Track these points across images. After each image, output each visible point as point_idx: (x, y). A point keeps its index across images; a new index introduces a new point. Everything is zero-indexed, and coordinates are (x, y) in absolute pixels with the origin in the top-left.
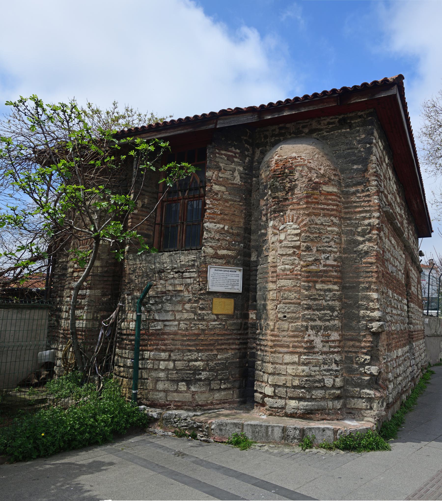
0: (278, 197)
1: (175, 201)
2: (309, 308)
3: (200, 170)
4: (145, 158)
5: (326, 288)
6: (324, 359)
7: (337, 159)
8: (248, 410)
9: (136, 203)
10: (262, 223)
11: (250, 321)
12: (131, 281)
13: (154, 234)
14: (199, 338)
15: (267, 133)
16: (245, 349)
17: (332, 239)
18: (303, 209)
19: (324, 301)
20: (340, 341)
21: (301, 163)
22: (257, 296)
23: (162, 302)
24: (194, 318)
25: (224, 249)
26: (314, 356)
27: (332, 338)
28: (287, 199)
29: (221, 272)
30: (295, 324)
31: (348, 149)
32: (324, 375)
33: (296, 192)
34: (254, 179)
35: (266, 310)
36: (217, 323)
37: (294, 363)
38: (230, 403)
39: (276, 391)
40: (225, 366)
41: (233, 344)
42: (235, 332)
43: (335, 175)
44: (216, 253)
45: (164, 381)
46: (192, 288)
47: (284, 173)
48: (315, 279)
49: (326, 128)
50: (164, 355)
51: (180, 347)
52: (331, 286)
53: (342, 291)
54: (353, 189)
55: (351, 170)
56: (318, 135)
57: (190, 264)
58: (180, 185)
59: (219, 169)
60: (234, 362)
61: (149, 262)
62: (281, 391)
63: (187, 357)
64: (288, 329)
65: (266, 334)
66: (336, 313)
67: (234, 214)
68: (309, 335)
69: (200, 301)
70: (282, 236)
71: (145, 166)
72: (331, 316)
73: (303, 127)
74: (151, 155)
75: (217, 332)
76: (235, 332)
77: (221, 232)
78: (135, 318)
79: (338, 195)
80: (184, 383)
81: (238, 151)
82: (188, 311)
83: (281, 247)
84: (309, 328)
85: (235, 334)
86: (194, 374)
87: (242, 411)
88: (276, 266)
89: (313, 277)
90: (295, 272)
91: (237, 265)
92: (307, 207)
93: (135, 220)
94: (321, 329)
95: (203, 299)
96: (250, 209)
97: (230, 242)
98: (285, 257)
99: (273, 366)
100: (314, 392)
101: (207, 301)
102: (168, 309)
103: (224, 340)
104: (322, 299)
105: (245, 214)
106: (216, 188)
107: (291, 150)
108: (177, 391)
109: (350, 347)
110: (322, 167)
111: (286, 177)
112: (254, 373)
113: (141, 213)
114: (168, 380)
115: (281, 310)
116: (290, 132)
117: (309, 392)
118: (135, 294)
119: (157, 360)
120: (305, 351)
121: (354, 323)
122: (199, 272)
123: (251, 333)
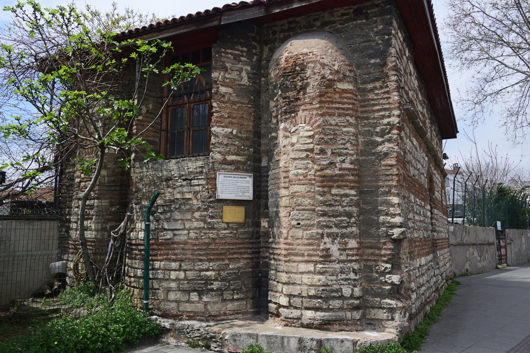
0: (288, 97)
1: (180, 106)
2: (324, 214)
3: (205, 70)
4: (147, 61)
5: (342, 193)
6: (341, 268)
7: (352, 53)
8: (262, 321)
9: (140, 109)
10: (272, 126)
11: (262, 230)
12: (138, 190)
13: (160, 141)
14: (210, 247)
15: (275, 29)
16: (258, 258)
17: (348, 141)
18: (316, 109)
19: (340, 207)
20: (358, 249)
21: (312, 59)
22: (269, 203)
23: (171, 211)
24: (204, 227)
25: (233, 154)
26: (331, 265)
27: (350, 246)
28: (298, 99)
29: (230, 179)
30: (310, 232)
31: (364, 42)
32: (342, 285)
33: (308, 90)
34: (263, 79)
35: (279, 217)
36: (227, 231)
37: (309, 272)
38: (243, 313)
39: (292, 301)
40: (237, 276)
41: (245, 253)
42: (247, 241)
43: (350, 71)
44: (225, 159)
45: (175, 291)
46: (201, 196)
47: (296, 70)
48: (330, 183)
49: (340, 20)
50: (174, 265)
51: (190, 256)
52: (347, 191)
53: (359, 196)
54: (370, 86)
55: (368, 65)
56: (331, 28)
57: (198, 171)
58: (185, 88)
59: (226, 69)
60: (246, 272)
61: (156, 170)
62: (297, 301)
63: (198, 267)
64: (303, 236)
65: (279, 243)
66: (353, 220)
67: (242, 117)
68: (325, 243)
69: (210, 209)
70: (294, 139)
71: (148, 69)
72: (348, 223)
73: (315, 20)
74: (154, 57)
75: (228, 241)
76: (247, 241)
77: (229, 136)
78: (143, 227)
79: (354, 92)
80: (195, 293)
81: (245, 49)
82: (197, 220)
83: (293, 151)
84: (325, 235)
85: (247, 243)
86: (206, 284)
87: (256, 322)
88: (288, 171)
89: (327, 182)
90: (309, 177)
91: (247, 171)
92: (320, 107)
93: (140, 127)
94: (337, 236)
95: (213, 207)
96: (260, 111)
97: (239, 147)
98: (297, 161)
99: (288, 276)
100: (331, 302)
101: (217, 209)
102: (177, 218)
103: (236, 249)
104: (338, 205)
105: (254, 117)
106: (223, 89)
107: (302, 45)
108: (189, 301)
109: (369, 255)
110: (336, 63)
111: (298, 76)
112: (268, 283)
113: (146, 119)
114: (179, 290)
115: (294, 217)
116: (300, 27)
117: (326, 302)
118: (143, 203)
119: (168, 270)
120: (321, 259)
121: (373, 230)
122: (208, 179)
123: (263, 242)
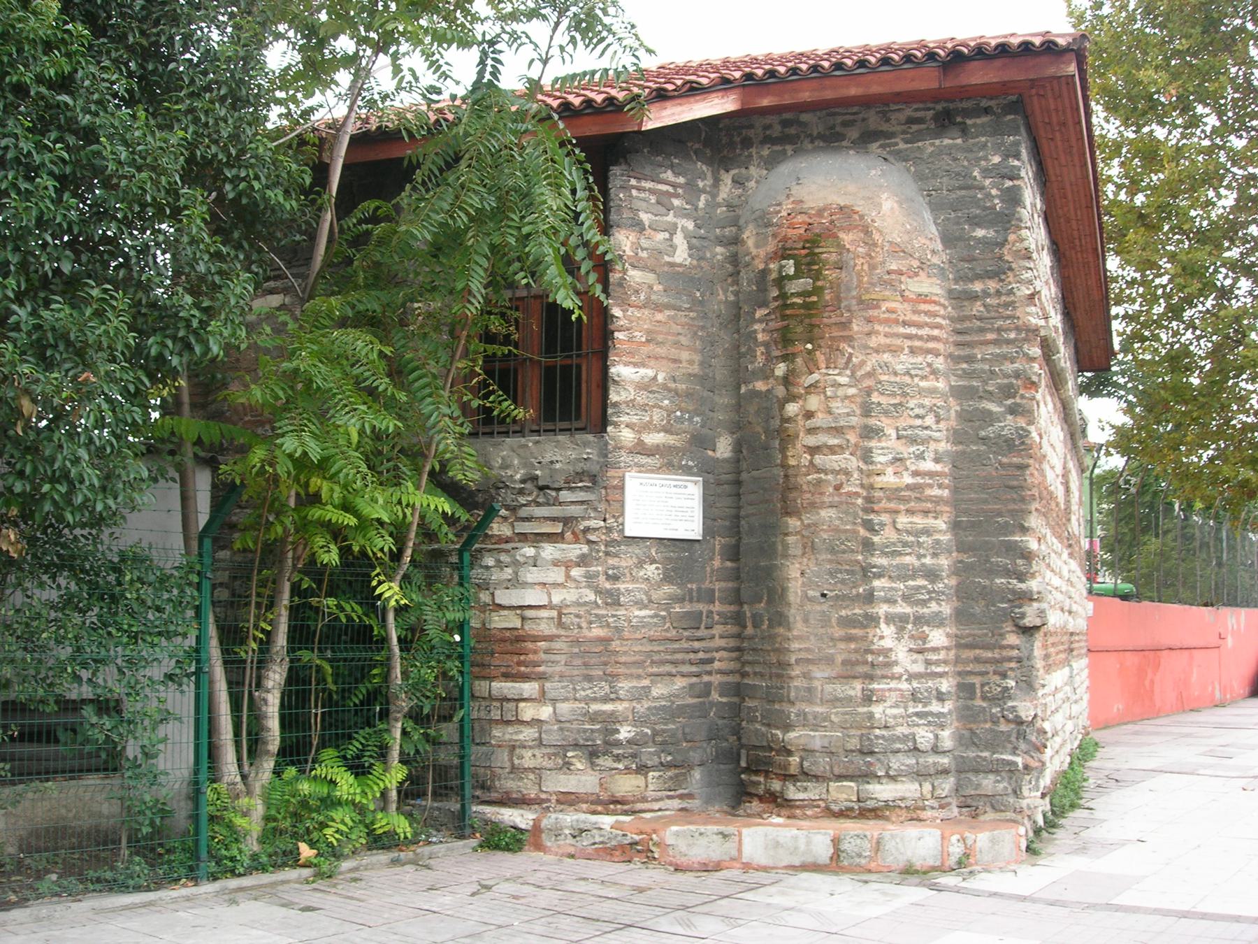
17: (931, 410)
31: (961, 188)
48: (892, 505)
49: (904, 132)
73: (845, 124)
81: (681, 180)
103: (666, 652)
104: (910, 554)
116: (811, 135)
